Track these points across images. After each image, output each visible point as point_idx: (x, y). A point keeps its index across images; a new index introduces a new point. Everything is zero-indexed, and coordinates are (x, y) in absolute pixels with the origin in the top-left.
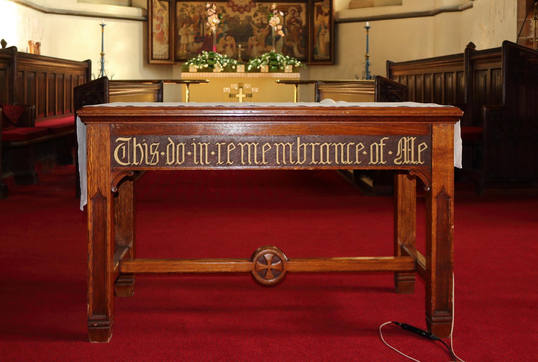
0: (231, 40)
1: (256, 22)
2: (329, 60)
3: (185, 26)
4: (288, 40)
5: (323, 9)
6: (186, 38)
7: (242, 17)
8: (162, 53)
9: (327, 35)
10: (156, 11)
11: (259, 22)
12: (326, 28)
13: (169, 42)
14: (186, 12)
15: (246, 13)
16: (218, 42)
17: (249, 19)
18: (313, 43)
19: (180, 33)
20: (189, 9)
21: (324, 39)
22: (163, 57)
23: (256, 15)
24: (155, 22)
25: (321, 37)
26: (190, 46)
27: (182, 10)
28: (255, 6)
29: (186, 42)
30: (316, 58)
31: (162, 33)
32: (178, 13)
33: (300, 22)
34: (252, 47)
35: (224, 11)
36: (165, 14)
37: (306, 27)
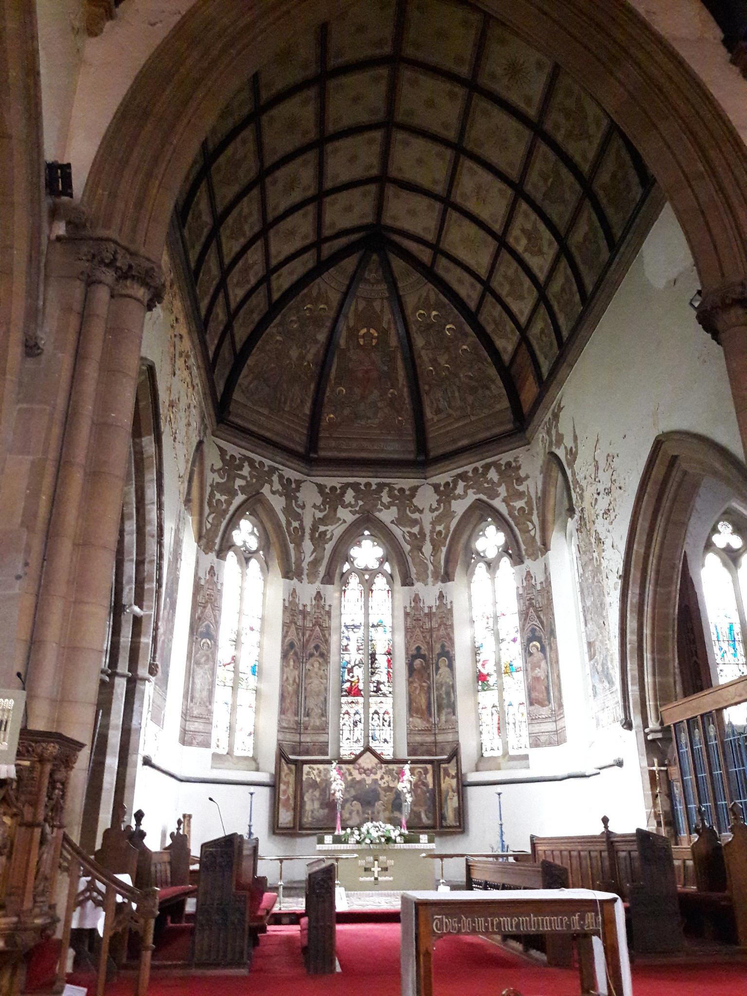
0: (357, 805)
1: (383, 785)
2: (459, 827)
3: (310, 791)
4: (415, 805)
5: (450, 771)
6: (312, 806)
7: (369, 781)
8: (286, 821)
9: (456, 799)
10: (283, 774)
11: (386, 785)
12: (453, 791)
13: (295, 809)
14: (312, 776)
15: (373, 776)
16: (343, 807)
17: (375, 781)
18: (441, 808)
19: (306, 799)
20: (315, 772)
21: (452, 803)
22: (288, 826)
23: (382, 778)
24: (283, 787)
25: (449, 801)
26: (315, 812)
27: (308, 773)
28: (381, 768)
29: (311, 808)
30: (444, 824)
31: (288, 798)
32: (305, 777)
33: (425, 785)
34: (378, 813)
35: (351, 774)
36: (292, 779)
37: (434, 790)
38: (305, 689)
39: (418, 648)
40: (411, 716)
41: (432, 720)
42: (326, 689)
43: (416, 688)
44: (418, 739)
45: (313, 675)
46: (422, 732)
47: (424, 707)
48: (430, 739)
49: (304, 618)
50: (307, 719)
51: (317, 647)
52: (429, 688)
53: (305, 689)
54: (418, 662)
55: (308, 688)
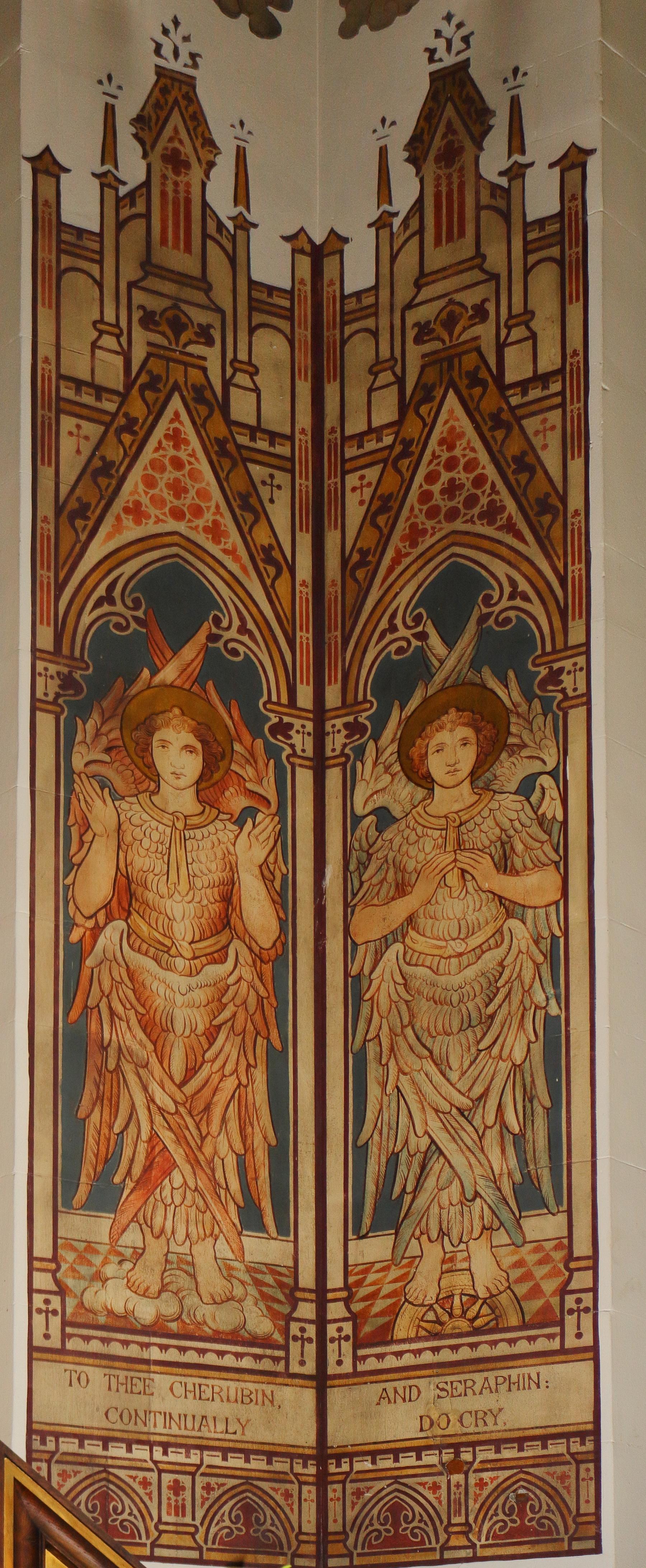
38: (356, 989)
42: (554, 955)
45: (424, 851)
49: (321, 364)
50: (375, 1248)
51: (452, 597)
53: (356, 989)
55: (384, 983)
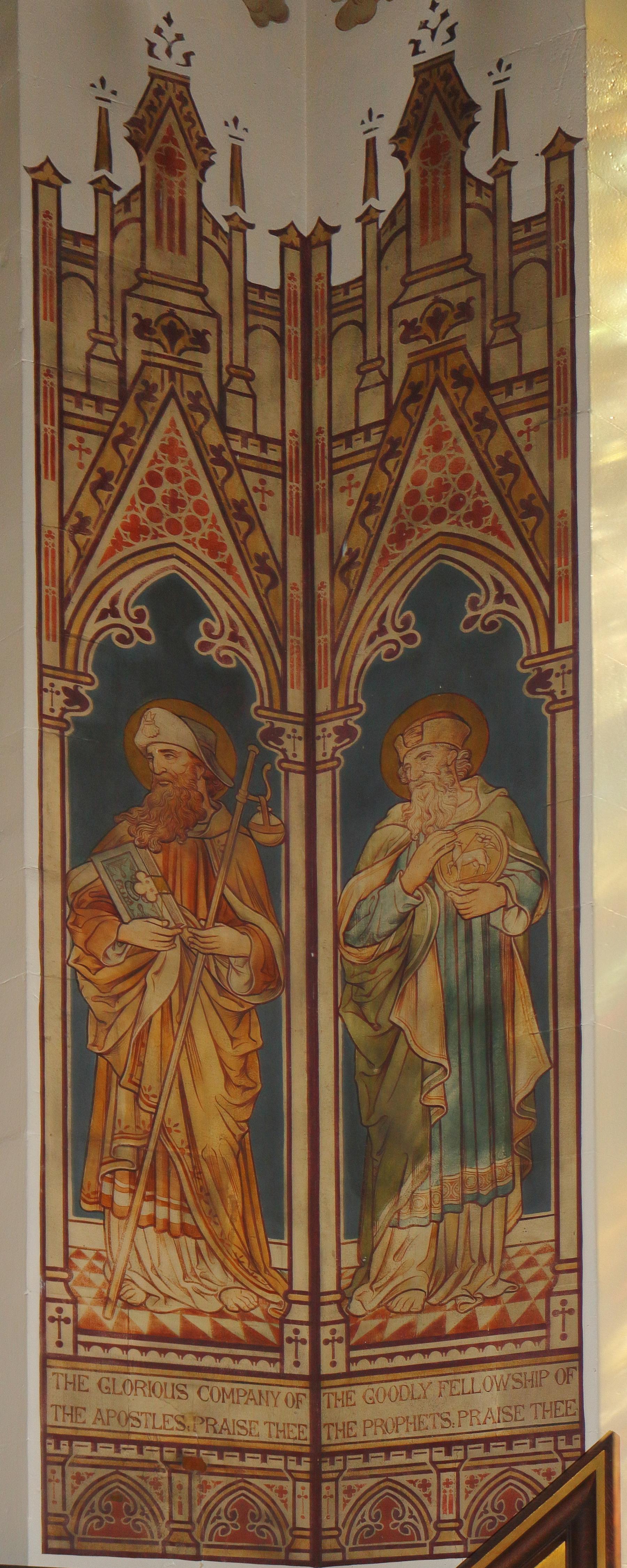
39: (174, 604)
40: (87, 1200)
41: (290, 1256)
43: (143, 962)
44: (156, 1409)
46: (184, 1349)
47: (216, 1136)
48: (271, 1415)
52: (270, 974)
54: (164, 733)
